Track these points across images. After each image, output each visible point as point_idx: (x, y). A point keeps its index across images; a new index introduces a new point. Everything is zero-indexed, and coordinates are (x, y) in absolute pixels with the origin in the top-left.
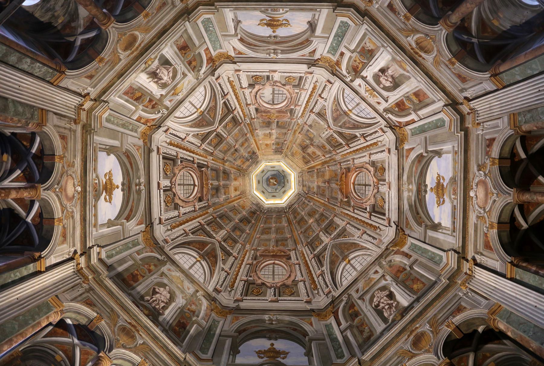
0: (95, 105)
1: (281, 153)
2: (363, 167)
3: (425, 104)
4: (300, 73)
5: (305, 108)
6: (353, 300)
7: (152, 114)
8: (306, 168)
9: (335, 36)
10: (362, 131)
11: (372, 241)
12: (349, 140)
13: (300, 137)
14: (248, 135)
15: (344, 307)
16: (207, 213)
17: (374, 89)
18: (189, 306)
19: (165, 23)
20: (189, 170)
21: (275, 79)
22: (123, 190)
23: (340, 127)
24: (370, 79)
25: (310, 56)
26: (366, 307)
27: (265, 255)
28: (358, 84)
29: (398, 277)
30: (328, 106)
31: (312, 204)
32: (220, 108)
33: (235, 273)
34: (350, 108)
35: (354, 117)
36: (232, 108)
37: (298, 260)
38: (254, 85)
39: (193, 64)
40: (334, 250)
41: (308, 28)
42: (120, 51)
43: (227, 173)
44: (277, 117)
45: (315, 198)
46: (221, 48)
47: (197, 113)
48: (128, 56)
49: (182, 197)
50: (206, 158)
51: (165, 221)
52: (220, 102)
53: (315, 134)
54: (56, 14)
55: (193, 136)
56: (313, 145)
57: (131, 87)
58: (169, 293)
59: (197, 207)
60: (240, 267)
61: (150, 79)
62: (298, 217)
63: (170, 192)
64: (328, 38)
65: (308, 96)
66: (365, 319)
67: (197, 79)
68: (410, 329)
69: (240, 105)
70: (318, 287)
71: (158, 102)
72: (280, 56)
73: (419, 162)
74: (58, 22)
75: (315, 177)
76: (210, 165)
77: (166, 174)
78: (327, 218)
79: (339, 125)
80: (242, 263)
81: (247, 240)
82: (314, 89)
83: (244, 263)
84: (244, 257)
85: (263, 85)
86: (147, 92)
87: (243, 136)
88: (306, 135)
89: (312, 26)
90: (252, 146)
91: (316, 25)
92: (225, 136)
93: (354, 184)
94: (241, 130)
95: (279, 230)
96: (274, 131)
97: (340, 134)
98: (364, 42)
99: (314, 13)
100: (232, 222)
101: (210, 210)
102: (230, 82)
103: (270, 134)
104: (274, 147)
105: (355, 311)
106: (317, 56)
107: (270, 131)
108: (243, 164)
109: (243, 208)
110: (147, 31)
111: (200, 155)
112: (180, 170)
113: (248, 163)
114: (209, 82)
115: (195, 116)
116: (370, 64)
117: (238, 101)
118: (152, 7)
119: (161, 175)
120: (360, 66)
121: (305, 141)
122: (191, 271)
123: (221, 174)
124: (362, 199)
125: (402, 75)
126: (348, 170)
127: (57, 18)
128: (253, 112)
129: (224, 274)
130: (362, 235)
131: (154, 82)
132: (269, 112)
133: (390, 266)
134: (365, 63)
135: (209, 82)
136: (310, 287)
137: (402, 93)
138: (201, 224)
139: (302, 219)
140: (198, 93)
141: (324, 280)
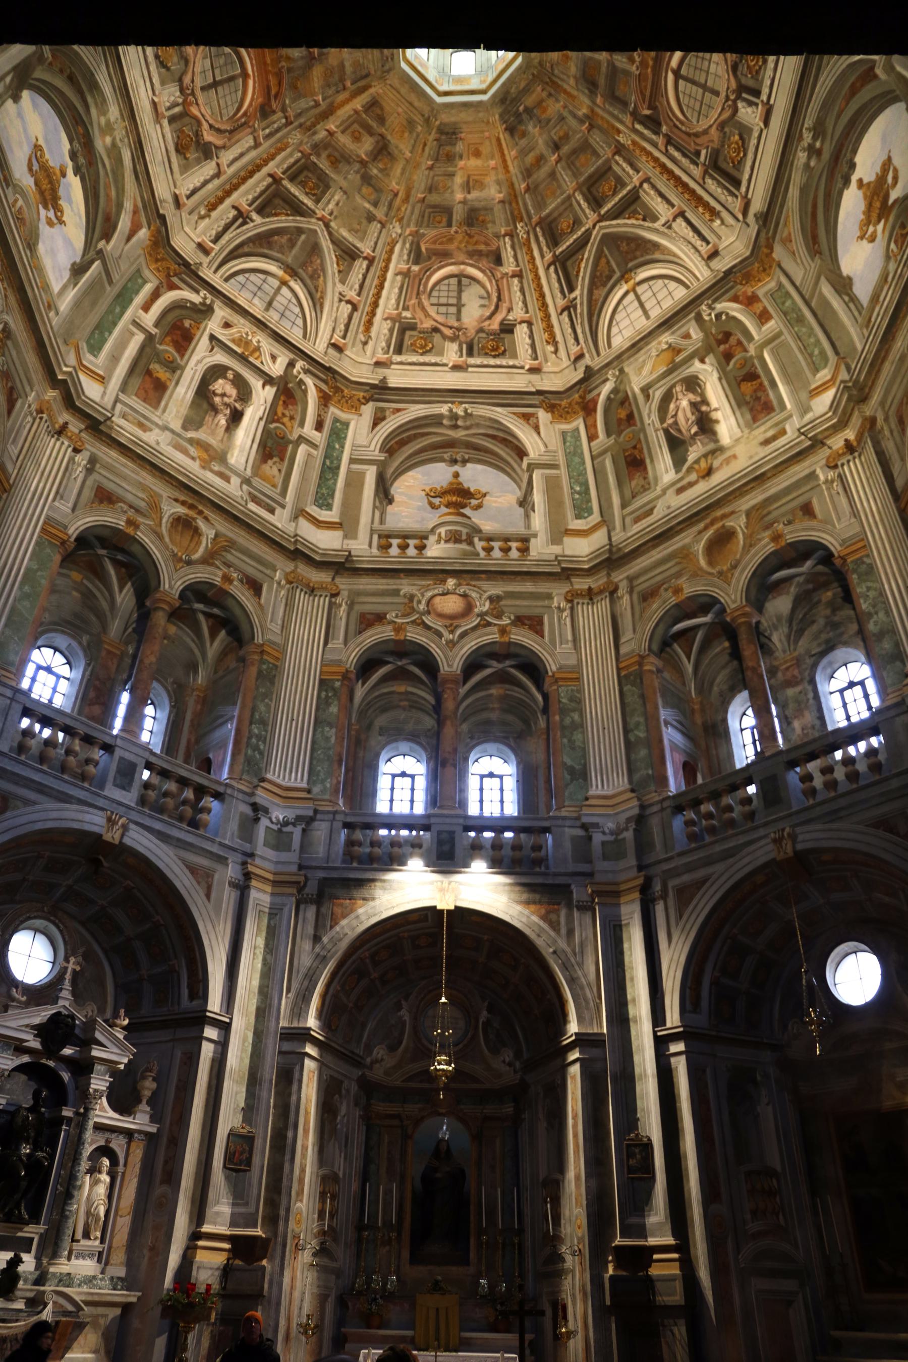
2: (231, 132)
3: (138, 371)
4: (401, 363)
5: (386, 268)
7: (734, 318)
9: (338, 468)
14: (523, 186)
17: (243, 359)
19: (654, 552)
20: (682, 123)
21: (455, 346)
23: (300, 231)
24: (256, 383)
25: (383, 410)
28: (279, 360)
30: (334, 284)
32: (583, 279)
34: (285, 291)
35: (272, 268)
36: (556, 271)
41: (392, 484)
42: (741, 536)
44: (451, 240)
46: (564, 434)
48: (733, 513)
50: (634, 143)
52: (579, 293)
53: (358, 199)
54: (828, 612)
55: (655, 219)
56: (363, 163)
57: (755, 419)
64: (352, 461)
65: (382, 302)
67: (622, 371)
69: (537, 277)
71: (713, 343)
72: (444, 409)
74: (834, 595)
75: (347, 64)
76: (628, 119)
79: (303, 237)
82: (369, 323)
85: (481, 330)
88: (378, 190)
90: (513, 153)
92: (579, 197)
93: (245, 75)
94: (540, 205)
96: (459, 196)
97: (298, 209)
99: (383, 527)
103: (467, 187)
104: (460, 147)
106: (368, 410)
107: (469, 197)
108: (542, 101)
110: (685, 554)
111: (649, 154)
113: (530, 101)
115: (643, 274)
116: (262, 423)
117: (540, 287)
118: (665, 602)
120: (280, 409)
121: (381, 171)
125: (198, 425)
128: (508, 254)
131: (708, 404)
132: (471, 254)
134: (274, 421)
135: (598, 354)
137: (188, 373)
140: (627, 333)
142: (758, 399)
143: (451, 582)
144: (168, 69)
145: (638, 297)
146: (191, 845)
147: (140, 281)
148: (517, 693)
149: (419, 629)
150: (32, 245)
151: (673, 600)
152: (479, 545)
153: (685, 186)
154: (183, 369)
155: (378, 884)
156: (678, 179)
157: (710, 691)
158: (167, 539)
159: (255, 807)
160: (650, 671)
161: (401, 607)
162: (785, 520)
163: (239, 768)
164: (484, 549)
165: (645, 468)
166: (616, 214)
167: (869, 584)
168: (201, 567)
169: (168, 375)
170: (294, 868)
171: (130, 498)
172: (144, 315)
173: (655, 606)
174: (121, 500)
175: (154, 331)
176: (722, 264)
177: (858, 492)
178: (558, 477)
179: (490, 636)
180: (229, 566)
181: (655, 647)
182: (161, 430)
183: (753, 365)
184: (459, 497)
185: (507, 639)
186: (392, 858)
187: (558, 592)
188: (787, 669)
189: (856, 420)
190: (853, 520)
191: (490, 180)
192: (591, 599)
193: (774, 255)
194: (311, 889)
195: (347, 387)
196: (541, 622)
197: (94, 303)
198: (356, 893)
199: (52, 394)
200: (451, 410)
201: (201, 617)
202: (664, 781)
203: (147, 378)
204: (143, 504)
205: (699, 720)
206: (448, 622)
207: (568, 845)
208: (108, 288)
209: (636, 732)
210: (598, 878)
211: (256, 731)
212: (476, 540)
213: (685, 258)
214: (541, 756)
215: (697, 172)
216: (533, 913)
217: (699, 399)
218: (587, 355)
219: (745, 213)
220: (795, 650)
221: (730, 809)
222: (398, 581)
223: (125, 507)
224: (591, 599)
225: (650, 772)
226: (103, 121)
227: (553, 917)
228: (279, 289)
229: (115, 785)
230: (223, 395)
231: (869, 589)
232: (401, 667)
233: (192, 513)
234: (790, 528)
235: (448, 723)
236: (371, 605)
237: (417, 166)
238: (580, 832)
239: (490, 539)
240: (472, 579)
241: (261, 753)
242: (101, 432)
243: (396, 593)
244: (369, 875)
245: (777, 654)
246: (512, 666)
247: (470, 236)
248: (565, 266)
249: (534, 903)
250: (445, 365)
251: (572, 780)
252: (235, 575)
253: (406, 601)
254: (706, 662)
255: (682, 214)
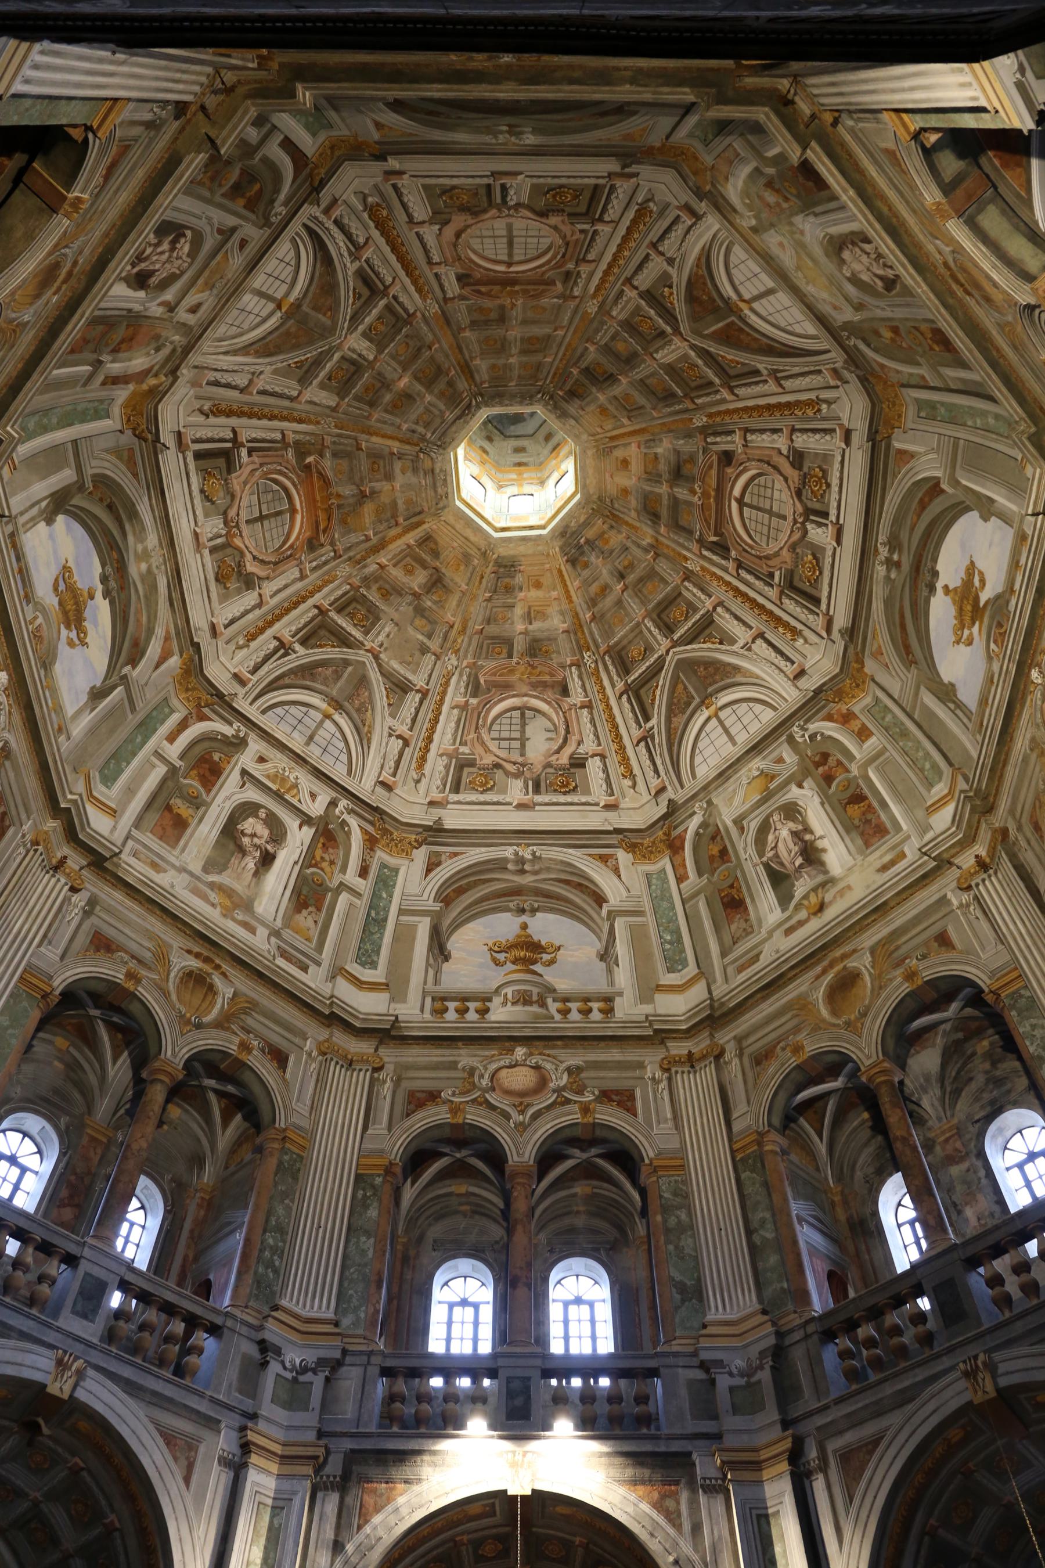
0: (953, 851)
1: (499, 563)
2: (276, 564)
3: (156, 805)
4: (459, 803)
5: (442, 701)
6: (253, 217)
7: (830, 737)
8: (430, 525)
9: (385, 920)
10: (291, 662)
11: (218, 376)
12: (321, 626)
13: (450, 614)
14: (588, 615)
15: (277, 191)
16: (710, 416)
17: (278, 796)
18: (785, 205)
19: (763, 1006)
21: (519, 783)
22: (935, 574)
23: (346, 663)
24: (291, 823)
25: (438, 854)
26: (209, 219)
27: (539, 283)
28: (319, 799)
29: (128, 326)
30: (383, 718)
31: (405, 427)
32: (660, 707)
33: (632, 244)
34: (328, 724)
35: (315, 700)
36: (629, 699)
37: (436, 275)
38: (572, 765)
39: (715, 849)
40: (329, 322)
41: (448, 939)
42: (867, 978)
43: (648, 513)
44: (512, 672)
45: (397, 444)
46: (648, 876)
47: (720, 703)
48: (854, 951)
49: (779, 483)
50: (703, 568)
51: (834, 430)
53: (411, 631)
54: (987, 1066)
55: (733, 641)
56: (416, 595)
57: (867, 844)
58: (843, 261)
59: (737, 438)
60: (616, 257)
61: (820, 844)
62: (441, 385)
63: (809, 504)
64: (401, 912)
65: (436, 737)
66: (207, 194)
67: (710, 803)
68: (73, 281)
70: (366, 215)
72: (508, 852)
73: (136, 644)
74: (991, 1044)
75: (400, 502)
76: (695, 547)
77: (815, 557)
78: (357, 398)
79: (350, 669)
80: (610, 266)
81: (595, 324)
82: (423, 759)
83: (603, 266)
84: (603, 280)
85: (548, 765)
86: (833, 809)
87: (603, 616)
88: (432, 622)
89: (439, 949)
90: (577, 583)
91: (430, 949)
92: (650, 624)
93: (293, 511)
94: (608, 634)
95: (502, 347)
96: (520, 627)
97: (344, 641)
98: (320, 924)
99: (437, 988)
100: (638, 377)
101: (700, 420)
102: (630, 774)
103: (529, 618)
104: (519, 579)
105: (243, 196)
106: (421, 855)
107: (530, 627)
108: (604, 533)
109: (603, 411)
110: (802, 1005)
111: (720, 578)
112: (777, 554)
113: (590, 533)
114: (682, 786)
115: (724, 698)
116: (297, 868)
117: (612, 718)
118: (783, 1065)
119: (828, 560)
120: (319, 853)
121: (435, 603)
122: (770, 284)
123: (664, 513)
124: (265, 476)
125: (222, 868)
126: (312, 545)
127: (988, 1055)
128: (575, 685)
129: (669, 246)
130: (251, 381)
131: (812, 832)
132: (534, 686)
133: (157, 337)
134: (311, 866)
135: (682, 786)
136: (389, 208)
137: (213, 811)
138: (731, 389)
139: (429, 384)
140: (713, 761)
141: (348, 236)
142: (868, 822)
143: (520, 1052)
144: (213, 503)
145: (721, 723)
146: (170, 1400)
147: (167, 710)
148: (606, 1190)
149: (482, 1110)
150: (47, 663)
151: (794, 1061)
152: (553, 1007)
153: (762, 607)
154: (208, 805)
155: (426, 1458)
156: (753, 601)
157: (852, 1177)
158: (174, 997)
159: (264, 1346)
160: (772, 1151)
161: (459, 1083)
162: (918, 954)
163: (245, 1291)
164: (559, 1011)
165: (746, 909)
166: (691, 638)
167: (1033, 1021)
168: (214, 1032)
169: (190, 811)
170: (311, 1436)
171: (133, 947)
172: (169, 745)
173: (771, 1070)
174: (120, 948)
175: (178, 763)
176: (809, 684)
177: (1000, 914)
178: (644, 925)
179: (571, 1116)
180: (249, 1032)
181: (776, 1121)
182: (180, 871)
183: (858, 786)
184: (528, 951)
185: (591, 1120)
186: (445, 1420)
187: (651, 1060)
188: (947, 1140)
189: (985, 835)
190: (1000, 947)
191: (553, 610)
192: (692, 1067)
193: (866, 670)
194: (334, 1467)
195: (397, 829)
196: (632, 1097)
197: (112, 731)
198: (396, 1473)
199: (52, 825)
200: (516, 854)
201: (212, 1097)
202: (803, 1297)
203: (166, 813)
204: (148, 955)
205: (841, 1214)
206: (517, 1100)
207: (683, 1392)
208: (130, 716)
209: (762, 1232)
210: (729, 1441)
211: (271, 1241)
212: (549, 1001)
213: (768, 678)
214: (641, 1274)
215: (773, 593)
216: (641, 1498)
217: (800, 827)
218: (669, 788)
219: (829, 630)
220: (953, 1116)
221: (897, 1331)
222: (455, 1052)
223: (126, 958)
224: (692, 1067)
225: (785, 1285)
226: (140, 547)
227: (670, 1503)
228: (322, 722)
229: (74, 1312)
230: (254, 835)
231: (1034, 1027)
232: (459, 1160)
233: (207, 968)
234: (926, 963)
235: (519, 1228)
236: (421, 1081)
237: (474, 597)
238: (700, 1375)
239: (566, 1000)
240: (546, 1047)
241: (276, 1272)
242: (106, 870)
243: (453, 1066)
244: (413, 1445)
245: (930, 1123)
246: (598, 1156)
247: (533, 667)
248: (638, 694)
249: (643, 1482)
250: (510, 804)
251: (683, 1301)
252: (256, 1043)
253: (466, 1075)
254: (843, 1139)
255: (761, 635)
